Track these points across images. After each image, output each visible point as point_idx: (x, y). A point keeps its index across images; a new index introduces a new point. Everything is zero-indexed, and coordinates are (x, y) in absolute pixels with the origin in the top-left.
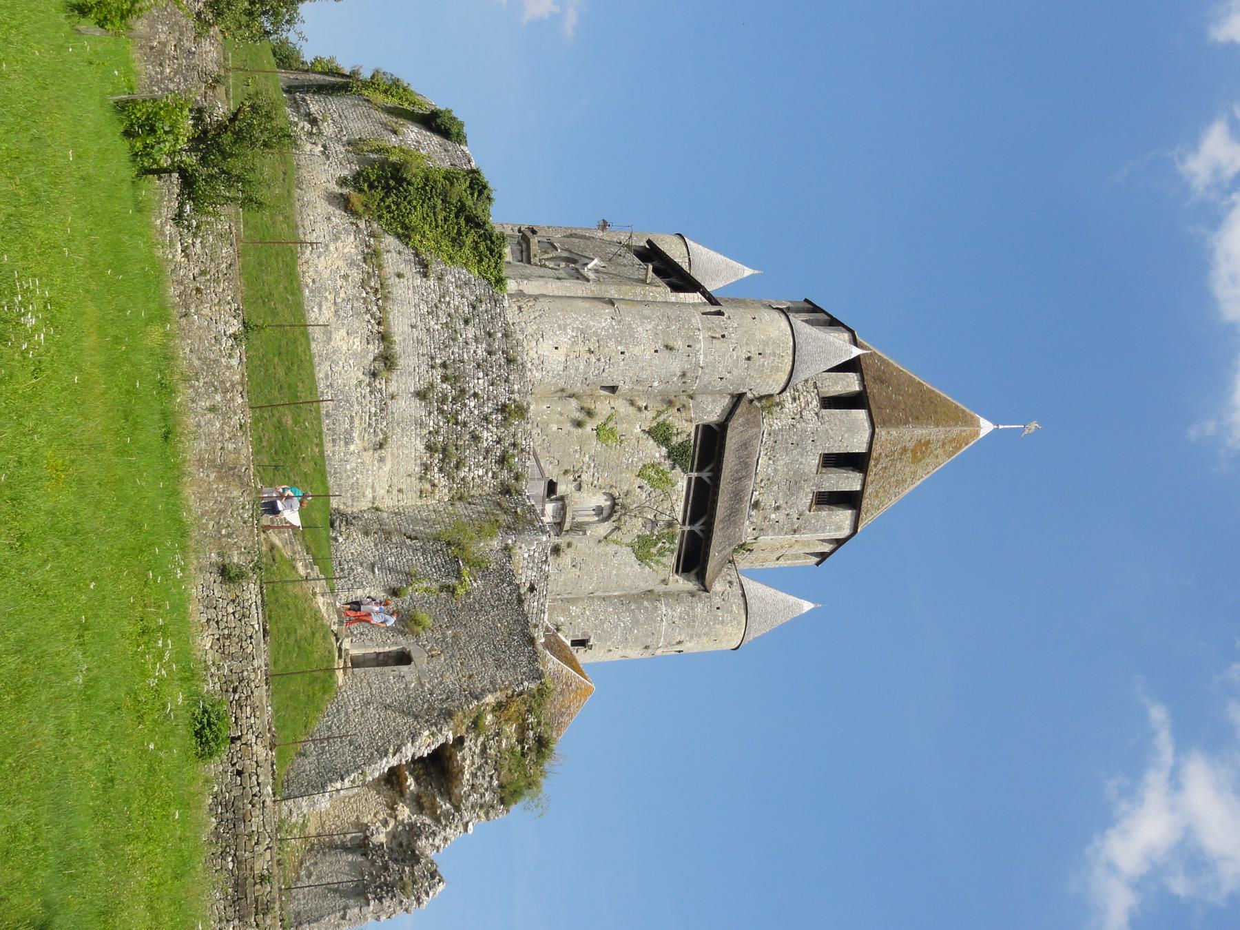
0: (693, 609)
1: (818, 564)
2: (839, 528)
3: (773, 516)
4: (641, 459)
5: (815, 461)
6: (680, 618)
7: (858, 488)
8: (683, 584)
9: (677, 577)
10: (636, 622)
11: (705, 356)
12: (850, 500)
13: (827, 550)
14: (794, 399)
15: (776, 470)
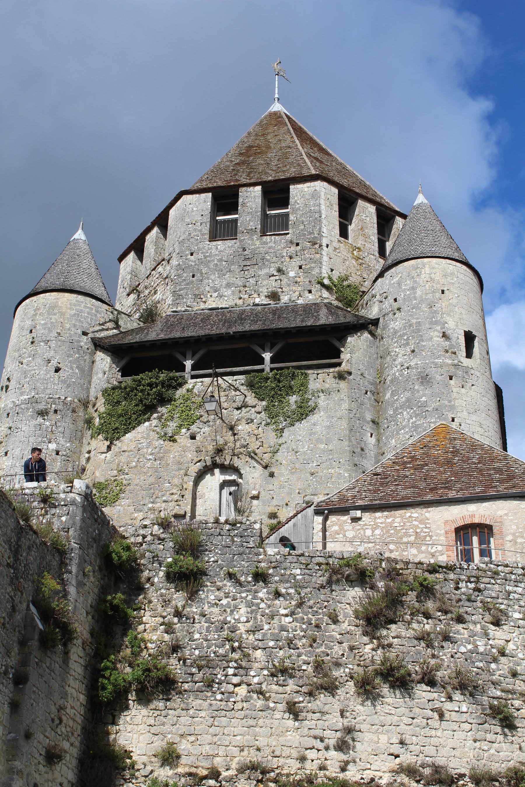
0: (396, 332)
1: (404, 216)
2: (315, 195)
3: (292, 274)
4: (149, 444)
5: (224, 247)
6: (407, 344)
7: (259, 188)
8: (356, 350)
9: (344, 364)
10: (409, 404)
11: (22, 394)
12: (276, 194)
13: (372, 209)
14: (155, 293)
15: (228, 285)
